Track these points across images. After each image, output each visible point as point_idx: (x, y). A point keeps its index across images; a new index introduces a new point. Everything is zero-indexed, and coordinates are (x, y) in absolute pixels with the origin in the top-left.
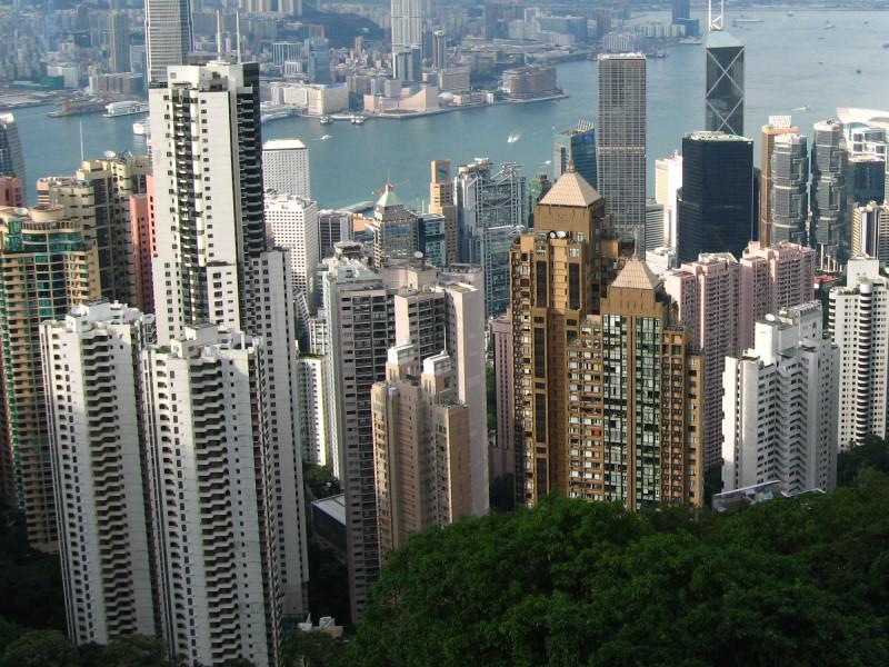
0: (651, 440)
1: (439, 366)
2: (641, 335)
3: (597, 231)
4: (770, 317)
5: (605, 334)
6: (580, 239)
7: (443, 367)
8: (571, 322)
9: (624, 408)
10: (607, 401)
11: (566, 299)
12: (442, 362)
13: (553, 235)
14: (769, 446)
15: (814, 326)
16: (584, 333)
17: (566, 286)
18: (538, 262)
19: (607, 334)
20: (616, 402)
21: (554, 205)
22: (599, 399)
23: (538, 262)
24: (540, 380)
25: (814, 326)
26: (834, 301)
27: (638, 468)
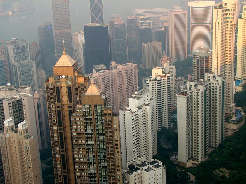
0: (103, 146)
1: (24, 126)
2: (97, 111)
3: (76, 74)
4: (133, 96)
5: (84, 112)
6: (70, 77)
7: (25, 126)
8: (70, 107)
9: (93, 136)
10: (86, 134)
11: (67, 99)
12: (25, 124)
13: (61, 77)
14: (137, 139)
15: (147, 96)
16: (76, 112)
17: (67, 94)
18: (56, 87)
19: (85, 112)
20: (89, 134)
21: (60, 67)
22: (83, 134)
23: (56, 87)
24: (61, 128)
25: (147, 96)
26: (148, 84)
27: (99, 156)
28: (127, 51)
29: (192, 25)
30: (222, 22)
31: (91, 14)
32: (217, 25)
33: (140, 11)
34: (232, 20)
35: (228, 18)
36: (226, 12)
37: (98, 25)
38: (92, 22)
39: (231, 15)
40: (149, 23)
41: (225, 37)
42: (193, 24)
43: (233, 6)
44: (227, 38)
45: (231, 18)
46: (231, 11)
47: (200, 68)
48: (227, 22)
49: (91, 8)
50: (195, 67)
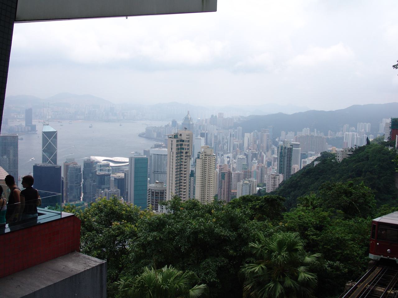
28: (82, 197)
29: (153, 173)
30: (176, 152)
31: (43, 155)
32: (172, 155)
33: (100, 159)
34: (187, 151)
35: (183, 149)
36: (181, 143)
37: (50, 165)
38: (43, 162)
39: (186, 146)
40: (109, 171)
41: (180, 168)
42: (155, 171)
43: (188, 137)
44: (182, 169)
45: (186, 150)
46: (186, 142)
47: (154, 203)
48: (182, 153)
49: (43, 148)
50: (149, 201)
